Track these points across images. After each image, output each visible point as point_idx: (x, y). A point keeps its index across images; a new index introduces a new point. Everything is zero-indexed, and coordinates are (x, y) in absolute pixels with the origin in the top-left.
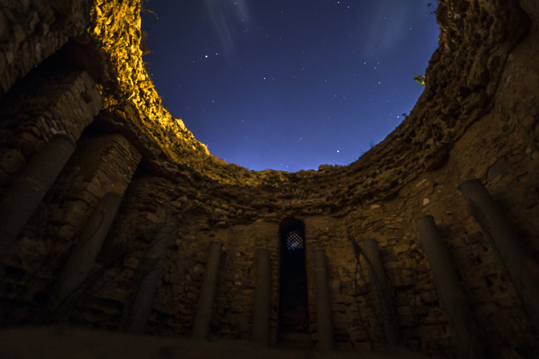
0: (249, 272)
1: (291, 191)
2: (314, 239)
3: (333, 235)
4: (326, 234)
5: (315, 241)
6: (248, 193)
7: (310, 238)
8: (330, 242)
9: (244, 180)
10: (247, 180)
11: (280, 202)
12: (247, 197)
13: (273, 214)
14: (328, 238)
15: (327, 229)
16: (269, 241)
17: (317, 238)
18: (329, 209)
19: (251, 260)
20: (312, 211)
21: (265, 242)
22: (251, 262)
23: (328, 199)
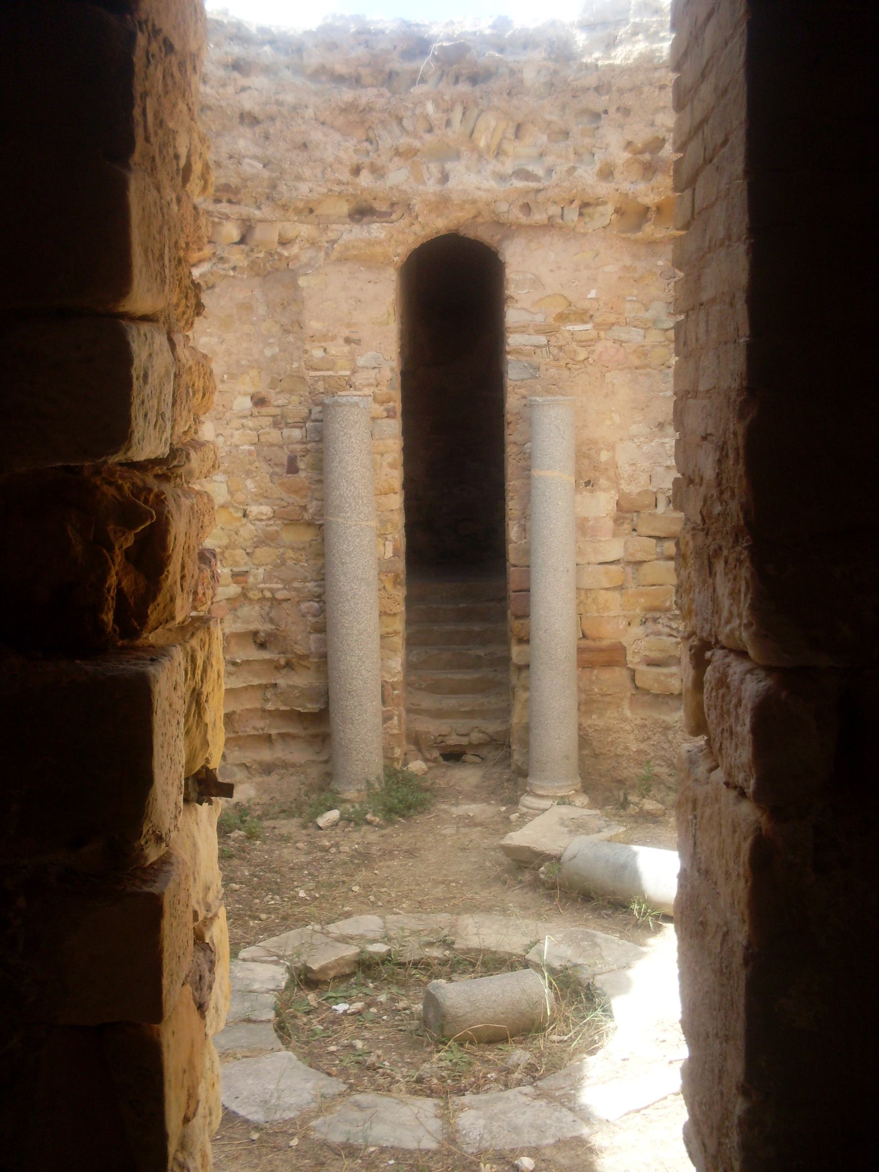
0: (292, 468)
1: (448, 123)
2: (539, 331)
3: (612, 318)
4: (583, 316)
5: (543, 340)
6: (254, 150)
7: (523, 329)
8: (599, 347)
9: (230, 90)
10: (244, 89)
11: (398, 176)
12: (250, 167)
13: (377, 230)
14: (594, 334)
15: (593, 294)
16: (358, 342)
17: (548, 331)
18: (610, 208)
19: (295, 426)
20: (539, 217)
21: (346, 349)
22: (297, 433)
23: (607, 173)
